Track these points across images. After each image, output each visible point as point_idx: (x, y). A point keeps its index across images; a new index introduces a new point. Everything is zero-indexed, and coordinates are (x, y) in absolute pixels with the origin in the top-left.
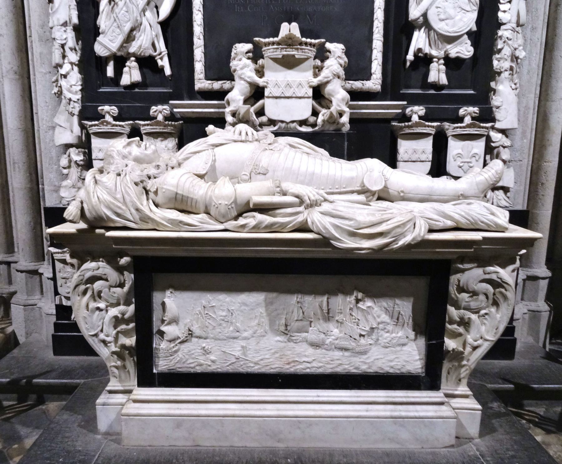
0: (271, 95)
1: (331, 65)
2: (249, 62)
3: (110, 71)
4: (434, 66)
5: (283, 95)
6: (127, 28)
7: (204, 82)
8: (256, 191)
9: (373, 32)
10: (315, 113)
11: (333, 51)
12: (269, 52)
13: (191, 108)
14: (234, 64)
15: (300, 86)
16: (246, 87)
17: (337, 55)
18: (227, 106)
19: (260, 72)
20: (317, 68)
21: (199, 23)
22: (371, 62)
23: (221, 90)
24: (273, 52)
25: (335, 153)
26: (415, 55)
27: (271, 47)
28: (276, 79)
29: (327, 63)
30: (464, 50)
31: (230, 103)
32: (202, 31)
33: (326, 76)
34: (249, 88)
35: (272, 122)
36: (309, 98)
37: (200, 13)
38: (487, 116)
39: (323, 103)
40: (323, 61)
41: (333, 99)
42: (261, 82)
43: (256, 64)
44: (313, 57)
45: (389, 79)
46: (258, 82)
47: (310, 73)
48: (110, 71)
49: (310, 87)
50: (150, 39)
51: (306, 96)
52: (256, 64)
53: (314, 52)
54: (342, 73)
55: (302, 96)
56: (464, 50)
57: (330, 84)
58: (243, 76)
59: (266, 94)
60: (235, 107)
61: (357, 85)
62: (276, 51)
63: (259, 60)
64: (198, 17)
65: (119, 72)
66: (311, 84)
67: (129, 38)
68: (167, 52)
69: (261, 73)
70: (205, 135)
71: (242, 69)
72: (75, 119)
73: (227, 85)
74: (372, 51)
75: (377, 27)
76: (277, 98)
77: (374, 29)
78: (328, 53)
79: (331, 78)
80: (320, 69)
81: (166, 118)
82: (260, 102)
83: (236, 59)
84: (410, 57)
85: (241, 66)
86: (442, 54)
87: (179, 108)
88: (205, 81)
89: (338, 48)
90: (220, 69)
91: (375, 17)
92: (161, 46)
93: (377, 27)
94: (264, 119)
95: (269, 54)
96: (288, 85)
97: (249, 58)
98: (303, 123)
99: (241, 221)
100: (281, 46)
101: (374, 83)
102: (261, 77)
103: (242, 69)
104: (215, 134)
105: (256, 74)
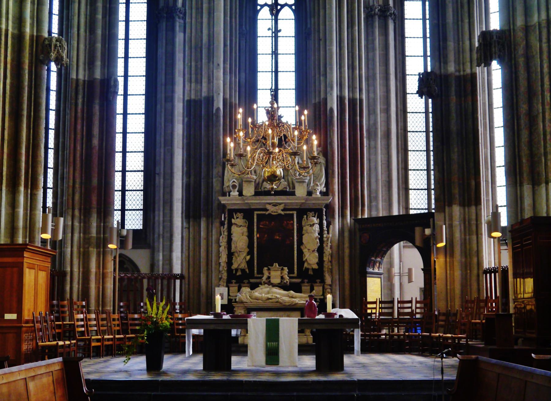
6: (239, 263)
8: (269, 296)
10: (281, 282)
14: (264, 272)
25: (285, 290)
30: (316, 267)
38: (323, 281)
50: (244, 265)
56: (316, 267)
61: (291, 275)
64: (256, 261)
67: (239, 265)
72: (225, 284)
90: (260, 272)
92: (246, 266)
98: (279, 284)
101: (295, 275)
104: (261, 287)
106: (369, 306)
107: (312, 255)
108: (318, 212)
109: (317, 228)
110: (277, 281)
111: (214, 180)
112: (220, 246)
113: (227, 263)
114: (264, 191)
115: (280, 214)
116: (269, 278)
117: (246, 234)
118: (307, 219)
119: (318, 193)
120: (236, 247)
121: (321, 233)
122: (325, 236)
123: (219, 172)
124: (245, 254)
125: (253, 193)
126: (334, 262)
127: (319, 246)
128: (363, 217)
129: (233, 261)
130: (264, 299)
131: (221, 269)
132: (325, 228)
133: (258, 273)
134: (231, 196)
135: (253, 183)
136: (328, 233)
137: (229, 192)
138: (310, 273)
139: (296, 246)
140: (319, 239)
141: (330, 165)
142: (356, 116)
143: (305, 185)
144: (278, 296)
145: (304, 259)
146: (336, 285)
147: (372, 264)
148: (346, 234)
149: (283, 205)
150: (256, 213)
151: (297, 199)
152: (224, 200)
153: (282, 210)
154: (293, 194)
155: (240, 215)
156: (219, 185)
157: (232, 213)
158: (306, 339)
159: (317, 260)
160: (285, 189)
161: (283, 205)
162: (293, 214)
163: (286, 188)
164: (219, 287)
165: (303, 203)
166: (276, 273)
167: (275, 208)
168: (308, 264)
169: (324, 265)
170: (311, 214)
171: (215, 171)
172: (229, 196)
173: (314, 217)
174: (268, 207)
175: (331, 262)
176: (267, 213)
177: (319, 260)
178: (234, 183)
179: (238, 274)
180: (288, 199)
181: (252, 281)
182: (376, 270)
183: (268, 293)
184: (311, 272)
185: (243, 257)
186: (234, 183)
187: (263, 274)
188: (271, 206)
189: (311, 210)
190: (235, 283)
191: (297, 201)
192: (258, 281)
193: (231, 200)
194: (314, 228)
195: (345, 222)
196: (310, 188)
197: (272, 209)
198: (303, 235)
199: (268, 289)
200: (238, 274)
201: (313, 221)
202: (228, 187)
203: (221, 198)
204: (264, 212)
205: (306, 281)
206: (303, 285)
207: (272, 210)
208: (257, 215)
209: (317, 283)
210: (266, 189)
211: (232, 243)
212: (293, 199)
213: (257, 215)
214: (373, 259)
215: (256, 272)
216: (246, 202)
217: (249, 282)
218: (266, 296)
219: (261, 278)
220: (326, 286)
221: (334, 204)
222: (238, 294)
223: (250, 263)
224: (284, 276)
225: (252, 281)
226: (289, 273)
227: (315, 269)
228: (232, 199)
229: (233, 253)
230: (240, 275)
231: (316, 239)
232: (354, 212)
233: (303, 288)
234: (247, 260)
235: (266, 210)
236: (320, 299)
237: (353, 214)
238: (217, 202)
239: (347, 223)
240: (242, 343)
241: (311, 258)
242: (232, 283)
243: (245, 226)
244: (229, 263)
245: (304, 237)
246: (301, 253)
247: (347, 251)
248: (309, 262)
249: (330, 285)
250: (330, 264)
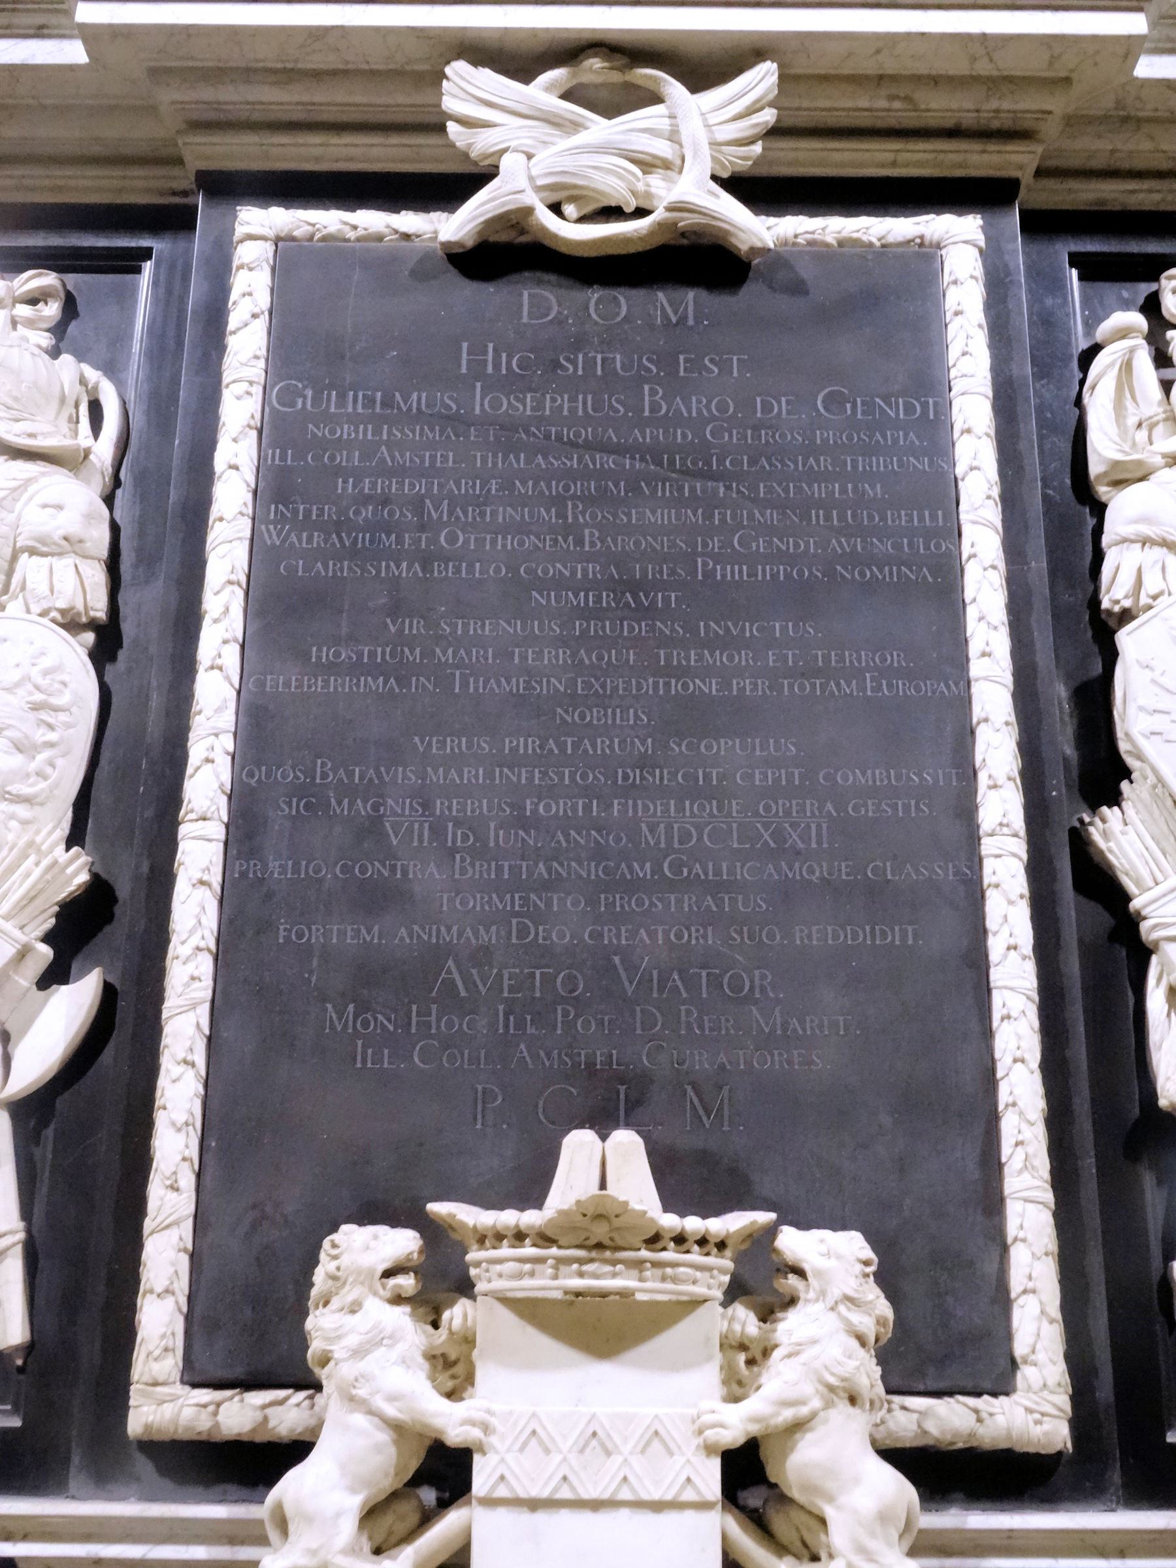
0: (502, 1492)
1: (814, 1342)
2: (400, 1316)
5: (565, 1494)
7: (174, 1399)
9: (1000, 1166)
11: (819, 1273)
12: (496, 1271)
13: (87, 1538)
14: (321, 1324)
15: (656, 1445)
16: (378, 1448)
17: (835, 1293)
18: (273, 1535)
19: (453, 1371)
20: (743, 1347)
21: (181, 1118)
22: (1003, 1301)
23: (258, 1439)
24: (520, 1276)
27: (505, 1251)
28: (530, 1407)
29: (791, 1326)
31: (292, 1528)
32: (194, 1152)
33: (792, 1394)
34: (392, 1451)
36: (703, 1506)
37: (190, 1074)
39: (780, 1523)
40: (767, 1315)
41: (829, 1512)
42: (453, 1421)
43: (436, 1325)
44: (719, 1294)
45: (1105, 1390)
46: (438, 1422)
47: (705, 1380)
49: (709, 1449)
51: (689, 1495)
52: (436, 1325)
53: (723, 1271)
55: (669, 1497)
57: (809, 1436)
58: (361, 1392)
59: (482, 1480)
60: (313, 1553)
62: (532, 1274)
63: (451, 1304)
66: (709, 1434)
68: (21, 1236)
69: (459, 1369)
71: (359, 1353)
73: (285, 1413)
74: (1005, 1249)
75: (1018, 1144)
76: (534, 1505)
77: (1006, 1150)
78: (793, 1279)
79: (816, 1403)
80: (759, 1357)
82: (452, 1520)
83: (335, 1303)
85: (352, 1340)
87: (25, 1537)
88: (180, 1389)
89: (839, 1257)
91: (1004, 1095)
93: (1018, 1144)
95: (498, 1284)
96: (595, 1440)
97: (397, 1299)
100: (554, 1251)
101: (1034, 1409)
102: (452, 1395)
103: (359, 1353)
105: (432, 1379)
115: (695, 260)
149: (761, 79)
150: (260, 222)
153: (740, 185)
162: (924, 258)
167: (599, 128)
176: (455, 226)
188: (542, 92)
204: (409, 221)
208: (289, 255)
219: (257, 1464)
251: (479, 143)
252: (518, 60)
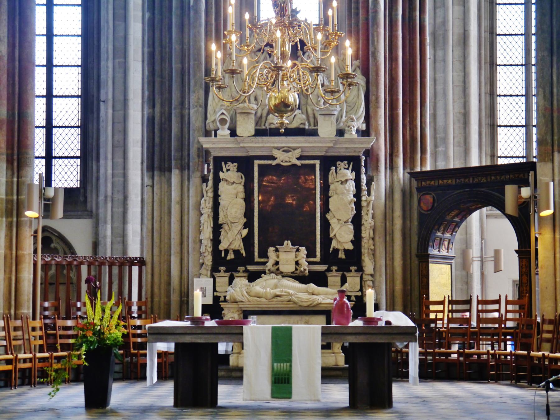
3: (223, 255)
4: (340, 252)
6: (231, 241)
8: (277, 292)
10: (296, 269)
12: (280, 250)
14: (269, 254)
25: (301, 282)
26: (333, 249)
30: (350, 247)
35: (282, 273)
38: (360, 269)
42: (278, 260)
48: (223, 255)
50: (238, 245)
54: (305, 256)
56: (350, 247)
65: (226, 255)
70: (261, 277)
72: (209, 273)
81: (244, 272)
84: (331, 249)
86: (343, 248)
90: (264, 254)
94: (279, 272)
98: (293, 273)
99: (273, 299)
101: (318, 259)
106: (432, 308)
107: (344, 228)
108: (354, 162)
109: (351, 186)
110: (288, 267)
111: (192, 111)
112: (202, 214)
113: (211, 240)
114: (270, 129)
115: (294, 165)
116: (277, 263)
117: (242, 195)
118: (336, 173)
119: (354, 133)
120: (226, 216)
121: (358, 195)
122: (364, 198)
123: (199, 99)
124: (241, 226)
125: (253, 133)
126: (377, 239)
127: (355, 215)
128: (424, 170)
129: (221, 238)
130: (269, 297)
131: (203, 249)
132: (364, 187)
133: (260, 257)
134: (218, 137)
135: (253, 116)
136: (369, 194)
137: (216, 131)
138: (340, 256)
139: (318, 215)
140: (355, 203)
141: (372, 88)
142: (415, 10)
143: (334, 119)
144: (291, 292)
145: (331, 235)
146: (380, 276)
147: (437, 242)
148: (398, 196)
149: (299, 151)
150: (257, 162)
151: (320, 142)
152: (207, 143)
153: (298, 159)
154: (314, 133)
155: (233, 166)
156: (201, 119)
157: (219, 162)
158: (334, 358)
159: (351, 237)
160: (302, 126)
161: (299, 151)
162: (314, 166)
163: (304, 124)
164: (199, 277)
165: (329, 147)
166: (289, 256)
167: (286, 154)
168: (338, 242)
169: (363, 244)
170: (342, 165)
171: (193, 98)
172: (216, 135)
173: (348, 169)
174: (276, 153)
175: (373, 239)
176: (274, 163)
177: (354, 236)
178: (223, 116)
179: (229, 258)
180: (306, 142)
181: (250, 268)
182: (444, 253)
183: (276, 287)
184: (342, 255)
185: (236, 232)
186: (223, 116)
187: (267, 257)
188: (280, 151)
189: (342, 158)
190: (225, 272)
191: (320, 145)
192: (260, 268)
193: (219, 143)
194: (347, 186)
195: (395, 178)
196: (342, 124)
197: (282, 158)
198: (330, 197)
199: (276, 281)
200: (229, 258)
201: (346, 175)
202: (213, 122)
203: (202, 140)
205: (334, 268)
206: (329, 274)
207: (282, 158)
208: (259, 166)
209: (351, 271)
210: (273, 126)
211: (220, 210)
212: (315, 142)
213: (259, 166)
214: (439, 234)
215: (256, 254)
216: (242, 145)
217: (246, 271)
218: (272, 291)
219: (264, 263)
220: (364, 276)
221: (379, 148)
222: (229, 288)
223: (248, 241)
224: (300, 262)
225: (250, 268)
226: (308, 256)
227: (348, 250)
228: (220, 144)
229: (221, 225)
230: (231, 259)
231: (350, 203)
232: (409, 160)
233: (330, 279)
234: (243, 236)
235: (274, 158)
236: (356, 297)
237: (408, 165)
238: (196, 146)
239: (399, 179)
240: (235, 364)
241: (343, 233)
242: (220, 271)
243: (240, 183)
244: (216, 241)
245: (330, 200)
246: (326, 225)
247: (398, 223)
248: (339, 239)
249: (372, 275)
250: (371, 242)
251: (276, 157)
252: (278, 149)
